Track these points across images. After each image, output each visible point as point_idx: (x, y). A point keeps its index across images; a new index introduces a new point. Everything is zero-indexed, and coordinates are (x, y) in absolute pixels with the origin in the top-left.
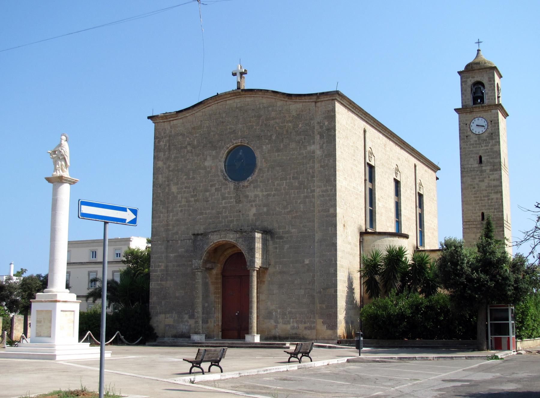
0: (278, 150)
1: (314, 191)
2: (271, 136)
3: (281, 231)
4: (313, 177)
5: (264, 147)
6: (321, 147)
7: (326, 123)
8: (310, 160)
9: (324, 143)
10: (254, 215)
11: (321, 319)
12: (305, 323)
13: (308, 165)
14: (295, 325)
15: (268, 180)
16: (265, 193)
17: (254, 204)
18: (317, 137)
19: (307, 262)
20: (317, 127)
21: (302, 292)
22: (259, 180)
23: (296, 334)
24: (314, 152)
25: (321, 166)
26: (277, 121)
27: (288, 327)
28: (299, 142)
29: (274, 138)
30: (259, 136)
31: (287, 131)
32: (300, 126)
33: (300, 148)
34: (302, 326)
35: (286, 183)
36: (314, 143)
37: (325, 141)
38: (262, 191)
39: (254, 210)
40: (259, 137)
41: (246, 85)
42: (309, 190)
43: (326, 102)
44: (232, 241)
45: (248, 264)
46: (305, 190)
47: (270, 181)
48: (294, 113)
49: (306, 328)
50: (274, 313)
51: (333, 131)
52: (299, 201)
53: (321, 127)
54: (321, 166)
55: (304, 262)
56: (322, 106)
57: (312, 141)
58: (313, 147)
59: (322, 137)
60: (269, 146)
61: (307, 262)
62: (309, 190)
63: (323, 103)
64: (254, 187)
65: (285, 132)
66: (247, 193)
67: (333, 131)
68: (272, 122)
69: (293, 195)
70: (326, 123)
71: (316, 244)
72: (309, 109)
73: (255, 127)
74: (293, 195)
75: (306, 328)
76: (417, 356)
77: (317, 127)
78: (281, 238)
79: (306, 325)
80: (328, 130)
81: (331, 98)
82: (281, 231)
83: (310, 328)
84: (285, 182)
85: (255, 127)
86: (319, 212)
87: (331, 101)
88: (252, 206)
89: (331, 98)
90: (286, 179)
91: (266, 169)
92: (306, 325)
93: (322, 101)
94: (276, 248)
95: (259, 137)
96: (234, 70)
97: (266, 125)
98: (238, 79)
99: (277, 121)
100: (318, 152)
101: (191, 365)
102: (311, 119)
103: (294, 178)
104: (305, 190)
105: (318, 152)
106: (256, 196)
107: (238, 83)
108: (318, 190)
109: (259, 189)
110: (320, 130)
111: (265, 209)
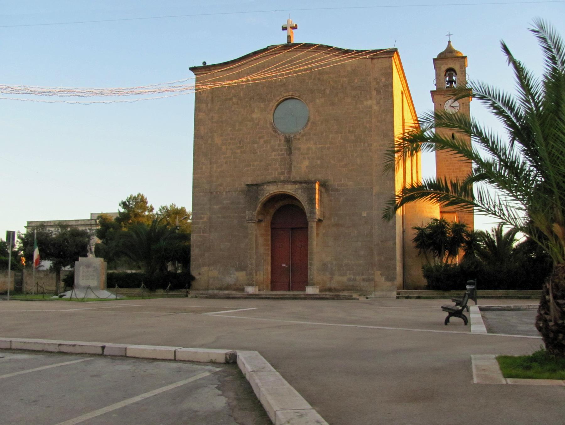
0: (333, 104)
1: (371, 145)
2: (325, 90)
3: (336, 183)
4: (370, 131)
5: (317, 101)
6: (378, 103)
7: (383, 80)
8: (367, 114)
9: (381, 99)
10: (307, 167)
11: (379, 270)
12: (363, 274)
13: (365, 120)
14: (352, 277)
15: (322, 133)
16: (318, 146)
17: (306, 156)
18: (374, 93)
19: (364, 214)
20: (374, 84)
21: (360, 244)
22: (312, 133)
23: (353, 286)
24: (371, 107)
25: (378, 121)
26: (331, 75)
27: (345, 279)
28: (355, 97)
29: (328, 92)
30: (311, 90)
31: (342, 86)
32: (356, 81)
33: (356, 103)
34: (358, 278)
35: (341, 136)
36: (371, 98)
37: (382, 97)
38: (315, 144)
39: (306, 163)
40: (312, 91)
41: (295, 40)
42: (366, 145)
43: (383, 59)
44: (291, 192)
45: (308, 215)
46: (362, 144)
47: (324, 134)
48: (349, 69)
49: (363, 280)
50: (329, 265)
51: (390, 87)
52: (355, 155)
53: (378, 83)
54: (378, 121)
55: (361, 214)
56: (380, 63)
57: (368, 97)
58: (369, 102)
59: (379, 92)
60: (323, 100)
61: (364, 214)
62: (366, 145)
63: (380, 60)
64: (307, 140)
65: (340, 87)
66: (300, 146)
67: (390, 87)
68: (326, 77)
69: (349, 149)
70: (383, 80)
71: (374, 197)
72: (365, 65)
73: (307, 81)
74: (349, 149)
75: (363, 280)
76: (512, 303)
77: (374, 84)
78: (337, 190)
79: (363, 277)
80: (385, 86)
81: (389, 56)
82: (336, 183)
83: (369, 280)
84: (340, 135)
85: (307, 81)
86: (376, 166)
87: (388, 59)
88: (304, 158)
89: (389, 56)
90: (341, 133)
91: (320, 123)
92: (363, 277)
93: (378, 58)
94: (331, 200)
95: (312, 91)
96: (284, 23)
97: (319, 79)
98: (288, 33)
99: (331, 75)
100: (376, 108)
101: (446, 314)
102: (368, 75)
103: (349, 132)
104: (362, 144)
105: (376, 108)
106: (309, 149)
107: (289, 37)
108: (375, 144)
109: (312, 142)
110: (377, 86)
111: (319, 162)
